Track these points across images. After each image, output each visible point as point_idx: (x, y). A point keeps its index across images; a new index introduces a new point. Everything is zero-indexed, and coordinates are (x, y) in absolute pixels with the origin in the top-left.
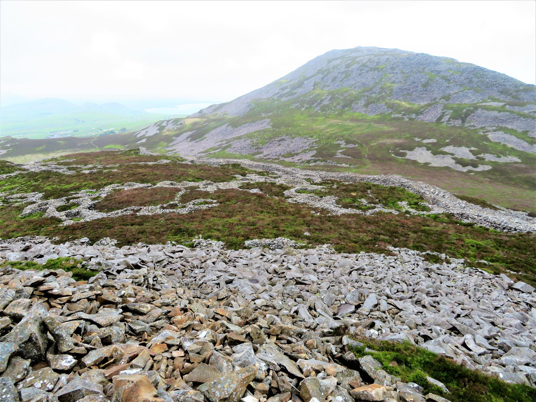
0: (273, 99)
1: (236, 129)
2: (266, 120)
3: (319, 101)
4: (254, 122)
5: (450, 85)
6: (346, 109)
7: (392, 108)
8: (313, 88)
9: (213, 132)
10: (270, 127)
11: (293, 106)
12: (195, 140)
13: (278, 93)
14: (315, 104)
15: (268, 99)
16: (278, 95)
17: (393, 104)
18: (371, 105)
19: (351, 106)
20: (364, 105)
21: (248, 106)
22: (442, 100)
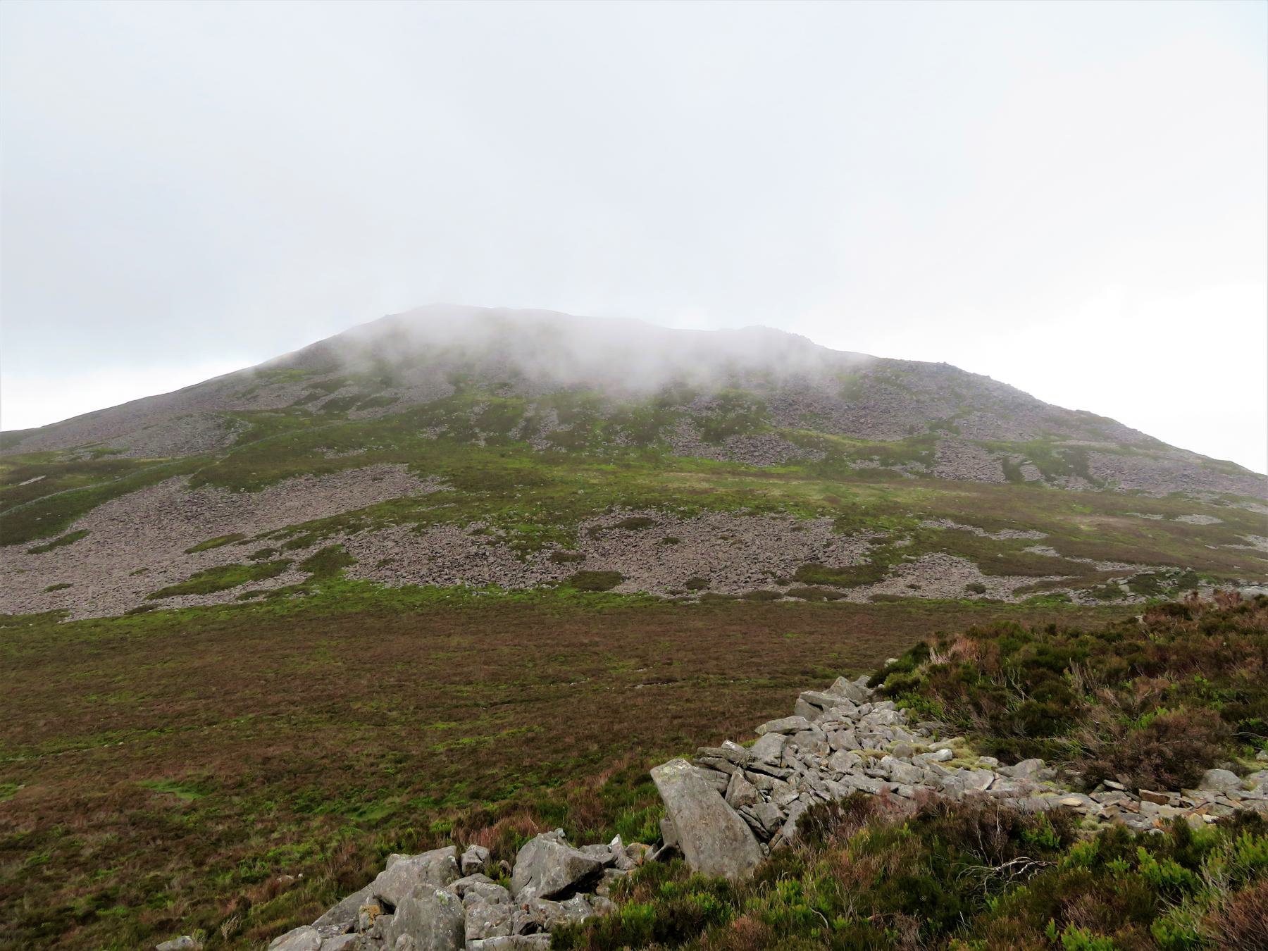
0: (306, 414)
1: (254, 496)
2: (386, 467)
3: (522, 423)
4: (330, 471)
5: (922, 398)
6: (652, 446)
7: (816, 447)
8: (454, 388)
9: (115, 507)
10: (444, 488)
11: (428, 434)
12: (22, 541)
13: (312, 398)
14: (514, 433)
15: (287, 411)
16: (320, 403)
17: (804, 437)
18: (729, 440)
19: (660, 441)
20: (705, 438)
21: (229, 425)
22: (940, 432)
